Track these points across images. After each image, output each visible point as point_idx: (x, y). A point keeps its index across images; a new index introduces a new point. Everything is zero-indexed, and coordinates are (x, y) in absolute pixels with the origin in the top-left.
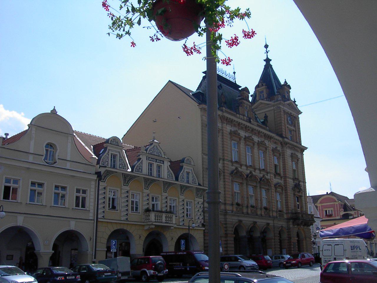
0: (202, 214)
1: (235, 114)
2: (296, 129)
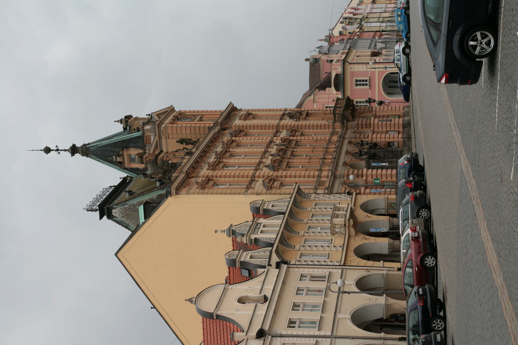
1: (180, 167)
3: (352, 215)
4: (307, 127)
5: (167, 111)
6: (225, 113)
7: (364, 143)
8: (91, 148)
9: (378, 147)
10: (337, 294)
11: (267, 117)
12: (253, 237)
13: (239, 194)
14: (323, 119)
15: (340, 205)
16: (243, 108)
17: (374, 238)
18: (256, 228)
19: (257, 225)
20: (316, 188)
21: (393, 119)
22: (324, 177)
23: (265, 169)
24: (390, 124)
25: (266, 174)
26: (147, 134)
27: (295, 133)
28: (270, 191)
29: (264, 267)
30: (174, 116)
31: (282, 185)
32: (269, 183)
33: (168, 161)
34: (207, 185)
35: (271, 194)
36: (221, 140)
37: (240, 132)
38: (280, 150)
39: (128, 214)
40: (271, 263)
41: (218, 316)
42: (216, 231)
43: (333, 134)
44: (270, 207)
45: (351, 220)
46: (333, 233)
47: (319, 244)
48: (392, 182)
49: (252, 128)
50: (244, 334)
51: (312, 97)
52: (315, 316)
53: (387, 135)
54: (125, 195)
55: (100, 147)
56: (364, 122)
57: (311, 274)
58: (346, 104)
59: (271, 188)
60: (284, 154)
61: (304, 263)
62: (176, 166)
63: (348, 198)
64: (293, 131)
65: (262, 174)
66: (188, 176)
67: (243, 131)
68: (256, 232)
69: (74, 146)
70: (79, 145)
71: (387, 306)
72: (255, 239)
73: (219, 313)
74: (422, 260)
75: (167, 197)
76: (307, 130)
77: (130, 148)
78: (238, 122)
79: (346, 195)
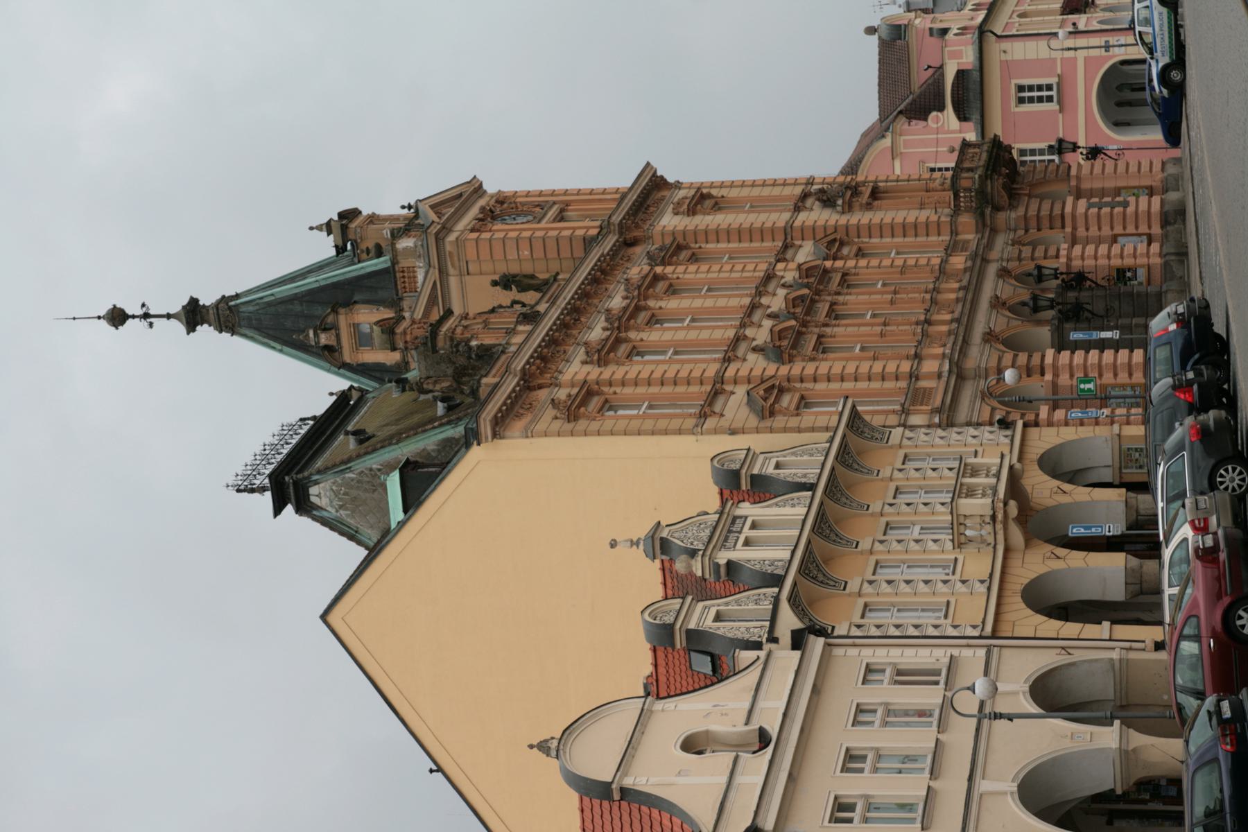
0: (955, 429)
1: (503, 358)
2: (554, 203)
3: (1015, 488)
4: (876, 231)
5: (461, 195)
6: (633, 197)
7: (1046, 272)
8: (243, 309)
9: (1089, 283)
10: (974, 721)
11: (756, 205)
12: (723, 557)
13: (680, 432)
14: (922, 206)
15: (979, 460)
16: (685, 179)
17: (1083, 554)
18: (730, 531)
19: (733, 522)
20: (905, 412)
21: (1132, 199)
22: (929, 376)
23: (752, 357)
24: (1124, 214)
25: (757, 372)
26: (404, 263)
27: (839, 249)
28: (768, 423)
29: (757, 646)
30: (482, 209)
31: (804, 403)
32: (765, 399)
33: (469, 340)
34: (583, 408)
35: (771, 430)
36: (620, 276)
37: (677, 249)
38: (795, 302)
39: (354, 499)
40: (777, 634)
41: (624, 791)
42: (613, 544)
43: (952, 248)
44: (770, 470)
45: (1012, 503)
46: (960, 543)
47: (919, 574)
48: (1133, 387)
49: (712, 237)
51: (887, 142)
52: (913, 787)
53: (1116, 249)
54: (344, 444)
55: (269, 304)
56: (1045, 212)
57: (895, 664)
58: (990, 158)
59: (772, 414)
60: (809, 313)
61: (874, 631)
62: (491, 356)
63: (1002, 437)
64: (834, 243)
65: (744, 372)
66: (528, 383)
67: (687, 247)
68: (731, 542)
69: (194, 302)
70: (207, 299)
71: (1127, 756)
72: (730, 564)
73: (628, 782)
74: (1229, 617)
75: (468, 446)
76: (875, 240)
77: (357, 306)
78: (669, 221)
79: (995, 428)
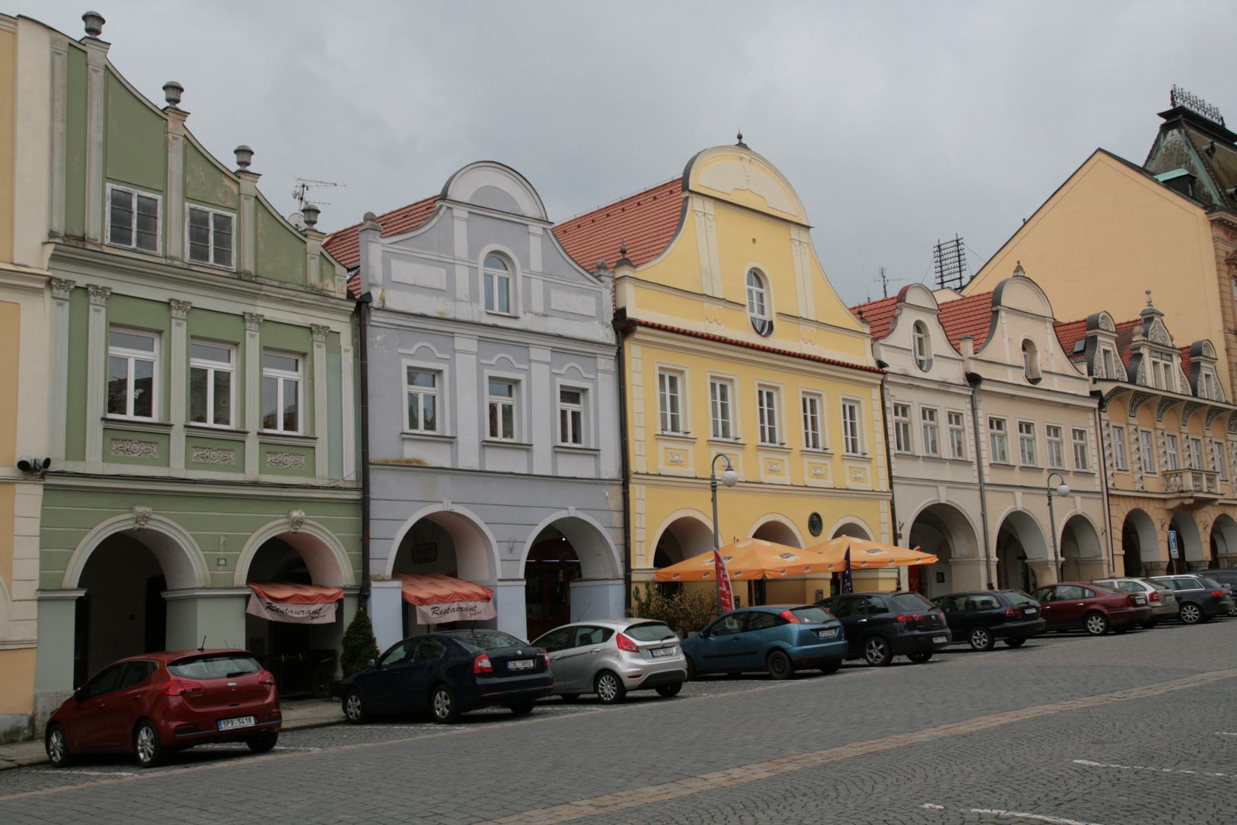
3: (1201, 503)
10: (1045, 486)
12: (1144, 351)
13: (1224, 321)
15: (1218, 482)
29: (1090, 373)
39: (1172, 154)
41: (997, 312)
42: (1148, 293)
44: (1204, 372)
45: (1192, 501)
46: (1166, 475)
47: (1144, 455)
50: (972, 355)
52: (1014, 457)
54: (1205, 142)
61: (1105, 433)
71: (1045, 564)
72: (1140, 355)
73: (1002, 314)
74: (1097, 613)
75: (1205, 208)
